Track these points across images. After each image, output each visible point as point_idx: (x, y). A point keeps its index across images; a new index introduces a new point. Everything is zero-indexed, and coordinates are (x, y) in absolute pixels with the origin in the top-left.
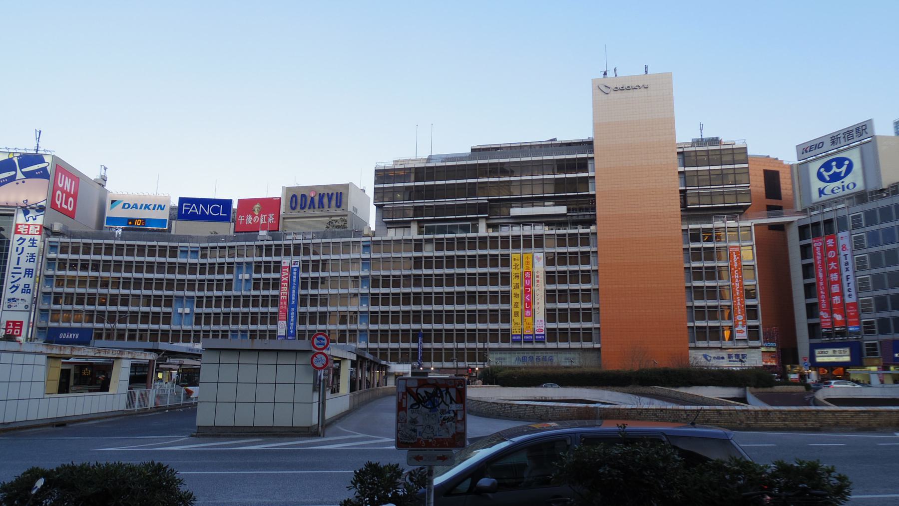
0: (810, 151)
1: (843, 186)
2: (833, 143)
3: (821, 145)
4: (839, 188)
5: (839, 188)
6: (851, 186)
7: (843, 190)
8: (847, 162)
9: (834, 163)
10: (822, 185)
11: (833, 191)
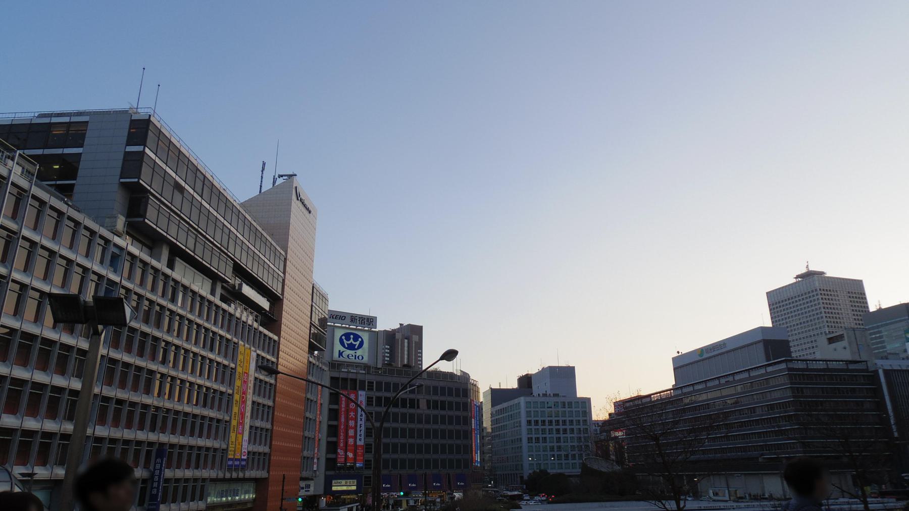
0: (335, 318)
1: (355, 356)
2: (352, 320)
3: (343, 318)
4: (353, 356)
5: (353, 356)
6: (360, 358)
7: (355, 358)
8: (360, 339)
9: (352, 336)
10: (342, 349)
11: (348, 356)
